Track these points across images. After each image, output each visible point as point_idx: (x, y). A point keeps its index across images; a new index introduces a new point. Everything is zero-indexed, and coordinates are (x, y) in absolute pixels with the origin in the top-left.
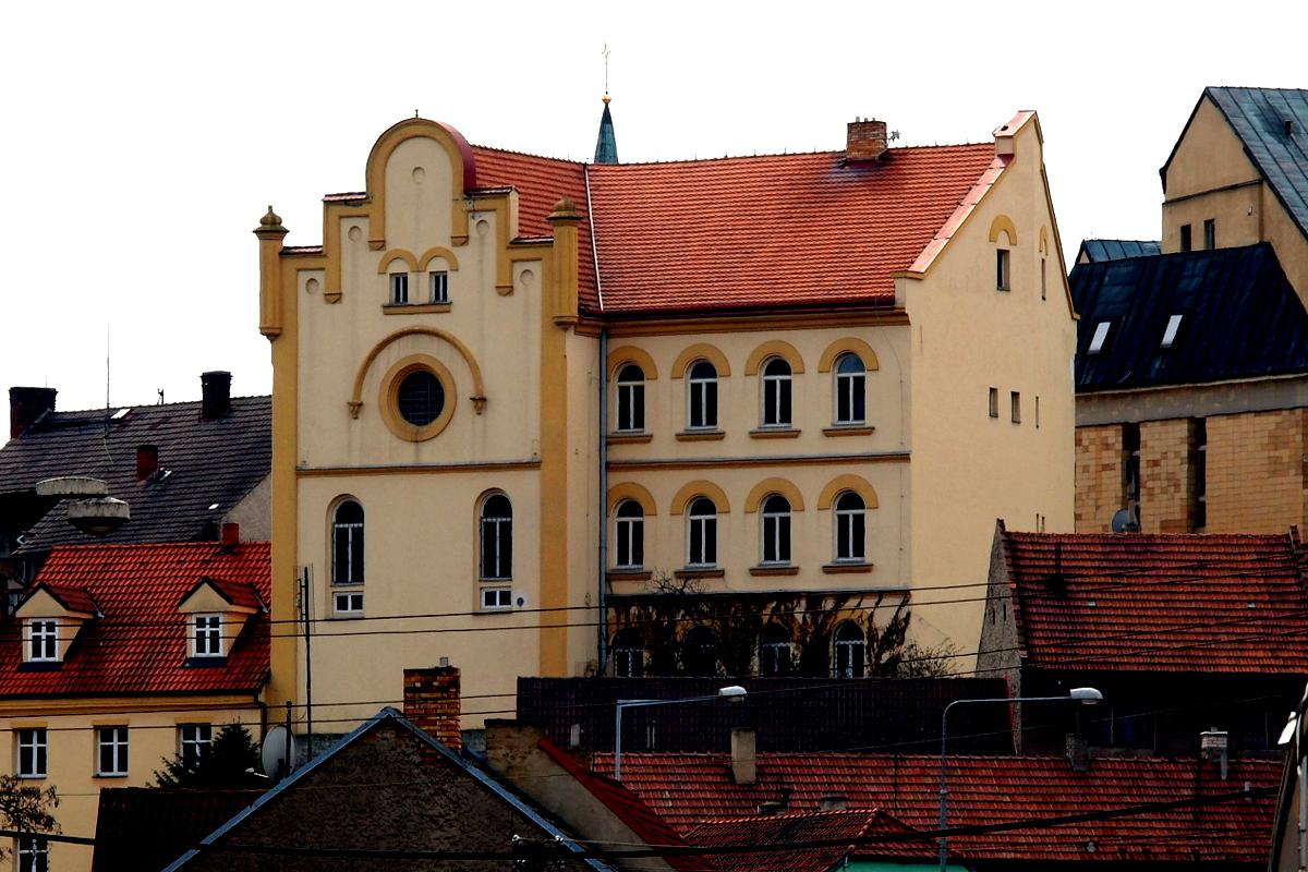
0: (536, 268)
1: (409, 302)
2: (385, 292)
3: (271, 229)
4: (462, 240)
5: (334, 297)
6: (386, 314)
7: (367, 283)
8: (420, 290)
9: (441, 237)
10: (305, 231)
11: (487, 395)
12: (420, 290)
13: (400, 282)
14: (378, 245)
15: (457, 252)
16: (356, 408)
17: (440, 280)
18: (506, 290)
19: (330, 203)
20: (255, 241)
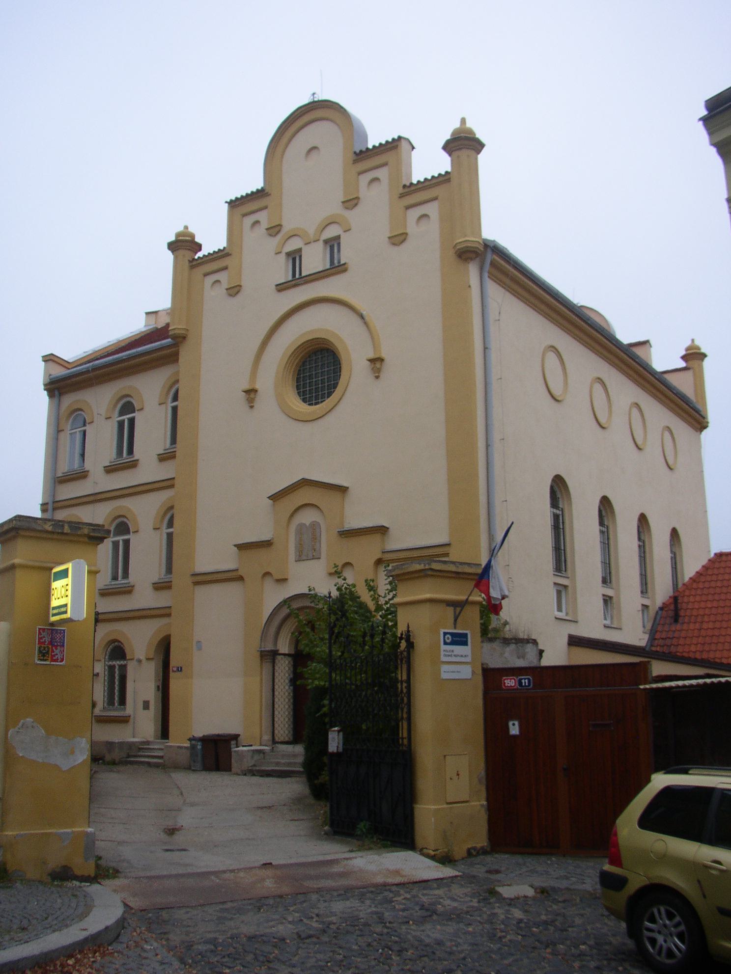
0: (432, 209)
1: (303, 274)
2: (281, 272)
3: (184, 245)
4: (351, 203)
5: (234, 291)
6: (279, 291)
7: (264, 265)
8: (314, 260)
9: (335, 208)
10: (213, 238)
11: (383, 355)
12: (314, 260)
13: (295, 257)
14: (274, 230)
15: (352, 216)
16: (251, 393)
17: (333, 244)
18: (398, 239)
19: (234, 204)
20: (169, 256)
